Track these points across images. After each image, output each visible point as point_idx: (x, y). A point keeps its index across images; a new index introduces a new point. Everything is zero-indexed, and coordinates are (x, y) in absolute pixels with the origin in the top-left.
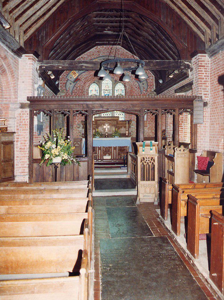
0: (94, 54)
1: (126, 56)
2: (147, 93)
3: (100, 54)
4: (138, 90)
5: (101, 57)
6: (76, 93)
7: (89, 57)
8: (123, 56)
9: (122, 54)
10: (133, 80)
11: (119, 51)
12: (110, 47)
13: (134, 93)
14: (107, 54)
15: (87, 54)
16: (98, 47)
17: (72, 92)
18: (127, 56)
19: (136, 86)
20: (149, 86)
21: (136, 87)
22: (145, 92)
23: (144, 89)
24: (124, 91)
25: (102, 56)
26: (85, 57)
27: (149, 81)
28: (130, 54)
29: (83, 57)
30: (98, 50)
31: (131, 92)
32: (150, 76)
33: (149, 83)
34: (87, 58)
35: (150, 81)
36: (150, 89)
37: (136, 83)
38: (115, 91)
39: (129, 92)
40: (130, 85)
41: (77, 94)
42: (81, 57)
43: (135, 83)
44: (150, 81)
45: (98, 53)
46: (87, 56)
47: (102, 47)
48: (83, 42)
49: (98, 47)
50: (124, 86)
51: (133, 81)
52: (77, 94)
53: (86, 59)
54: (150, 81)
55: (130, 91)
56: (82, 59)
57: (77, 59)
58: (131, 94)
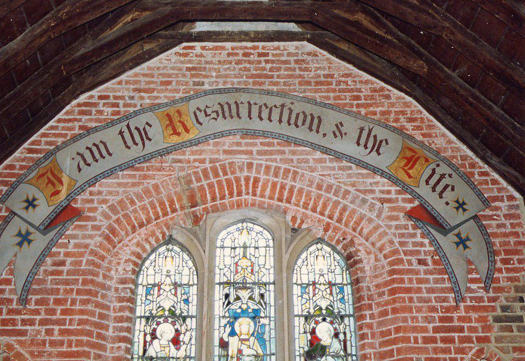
0: (169, 83)
1: (344, 91)
2: (494, 300)
3: (203, 84)
4: (436, 281)
5: (206, 93)
6: (52, 297)
7: (142, 98)
8: (328, 91)
9: (321, 83)
10: (397, 219)
11: (306, 69)
12: (257, 47)
13: (414, 296)
14: (239, 83)
15: (137, 82)
16: (192, 48)
17: (27, 290)
18: (350, 91)
19: (422, 257)
20: (503, 256)
21: (421, 262)
22: (481, 293)
23: (470, 272)
24: (348, 290)
25: (213, 92)
26: (118, 94)
27: (494, 223)
28: (367, 82)
29: (107, 97)
30: (190, 62)
31: (393, 292)
32: (496, 199)
33: (496, 235)
34: (132, 98)
35: (504, 226)
36: (508, 270)
37: (419, 239)
38: (297, 290)
39: (381, 294)
40: (381, 250)
41: (58, 302)
42: (101, 98)
43: (414, 235)
44: (504, 226)
45: (193, 76)
46: (135, 90)
47: (216, 48)
48: (120, 42)
49: (192, 48)
50: (349, 257)
51: (397, 227)
52: (58, 302)
53: (125, 105)
54: (499, 226)
55: (386, 284)
56: (104, 104)
57: (74, 102)
58: (394, 301)
